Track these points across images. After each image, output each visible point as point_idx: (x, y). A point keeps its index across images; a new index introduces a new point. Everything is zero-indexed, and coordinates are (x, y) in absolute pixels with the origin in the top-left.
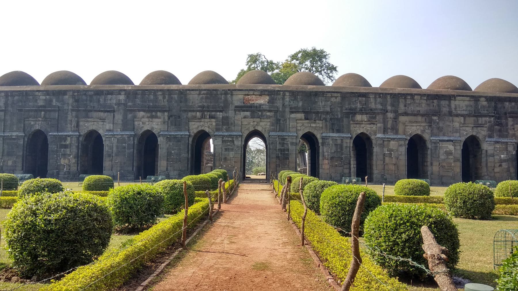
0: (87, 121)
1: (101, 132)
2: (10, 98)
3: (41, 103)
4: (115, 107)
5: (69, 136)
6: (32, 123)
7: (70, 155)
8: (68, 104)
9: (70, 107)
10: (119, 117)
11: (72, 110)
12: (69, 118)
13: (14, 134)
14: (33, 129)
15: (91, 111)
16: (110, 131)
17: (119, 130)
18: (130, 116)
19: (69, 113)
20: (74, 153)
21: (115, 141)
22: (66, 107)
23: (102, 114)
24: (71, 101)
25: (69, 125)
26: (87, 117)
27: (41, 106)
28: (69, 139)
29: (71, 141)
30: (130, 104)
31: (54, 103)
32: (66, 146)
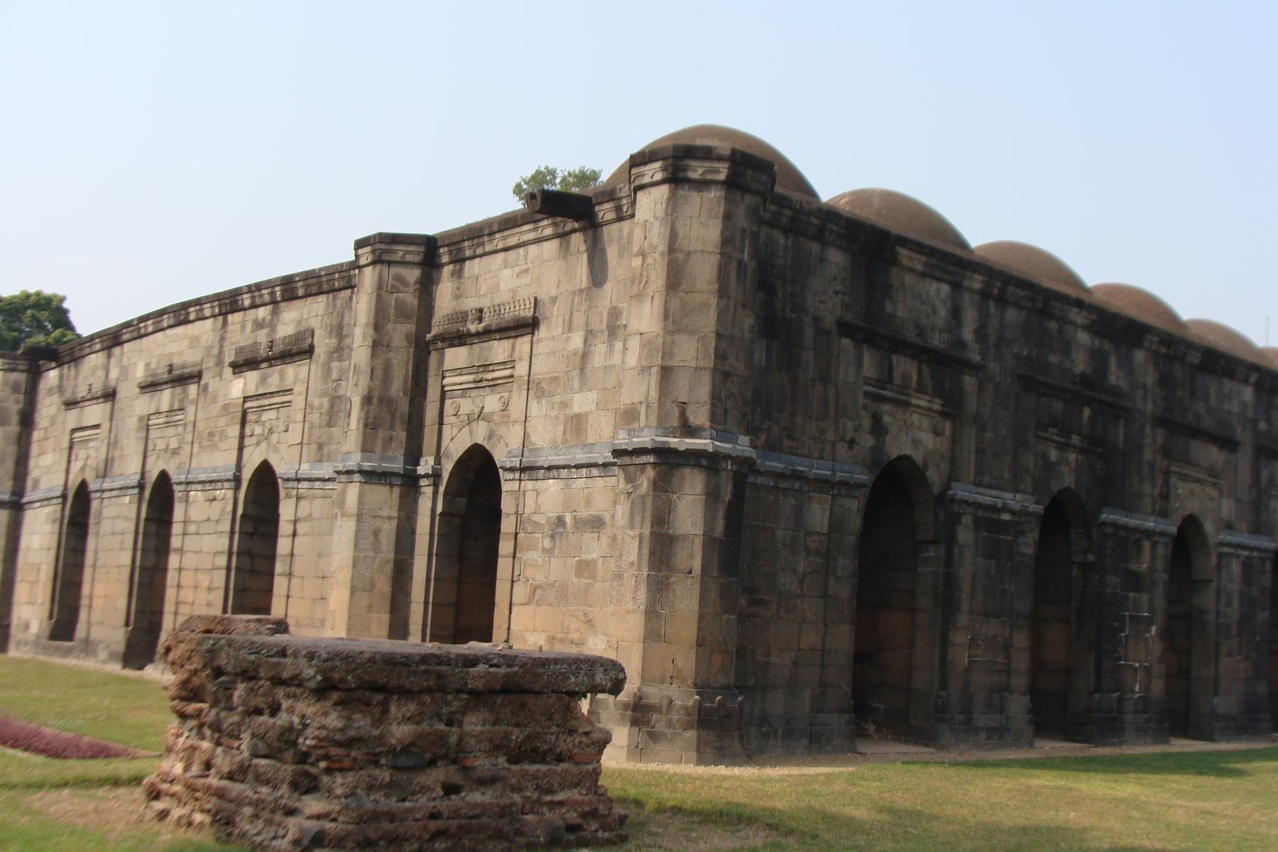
0: (1185, 478)
1: (1209, 527)
2: (992, 308)
3: (1080, 363)
4: (1239, 430)
5: (1149, 534)
6: (1053, 454)
7: (1150, 621)
8: (1144, 386)
9: (1150, 407)
10: (1244, 475)
11: (1159, 421)
12: (1148, 455)
13: (1013, 500)
14: (1055, 487)
15: (1196, 433)
16: (1229, 526)
17: (1244, 526)
18: (1265, 474)
19: (1148, 431)
20: (1160, 617)
21: (1236, 568)
22: (1139, 404)
23: (1213, 455)
24: (1150, 378)
25: (1147, 488)
26: (1186, 460)
27: (1086, 381)
28: (1146, 545)
29: (1153, 558)
30: (1262, 426)
31: (1115, 377)
32: (1135, 582)
